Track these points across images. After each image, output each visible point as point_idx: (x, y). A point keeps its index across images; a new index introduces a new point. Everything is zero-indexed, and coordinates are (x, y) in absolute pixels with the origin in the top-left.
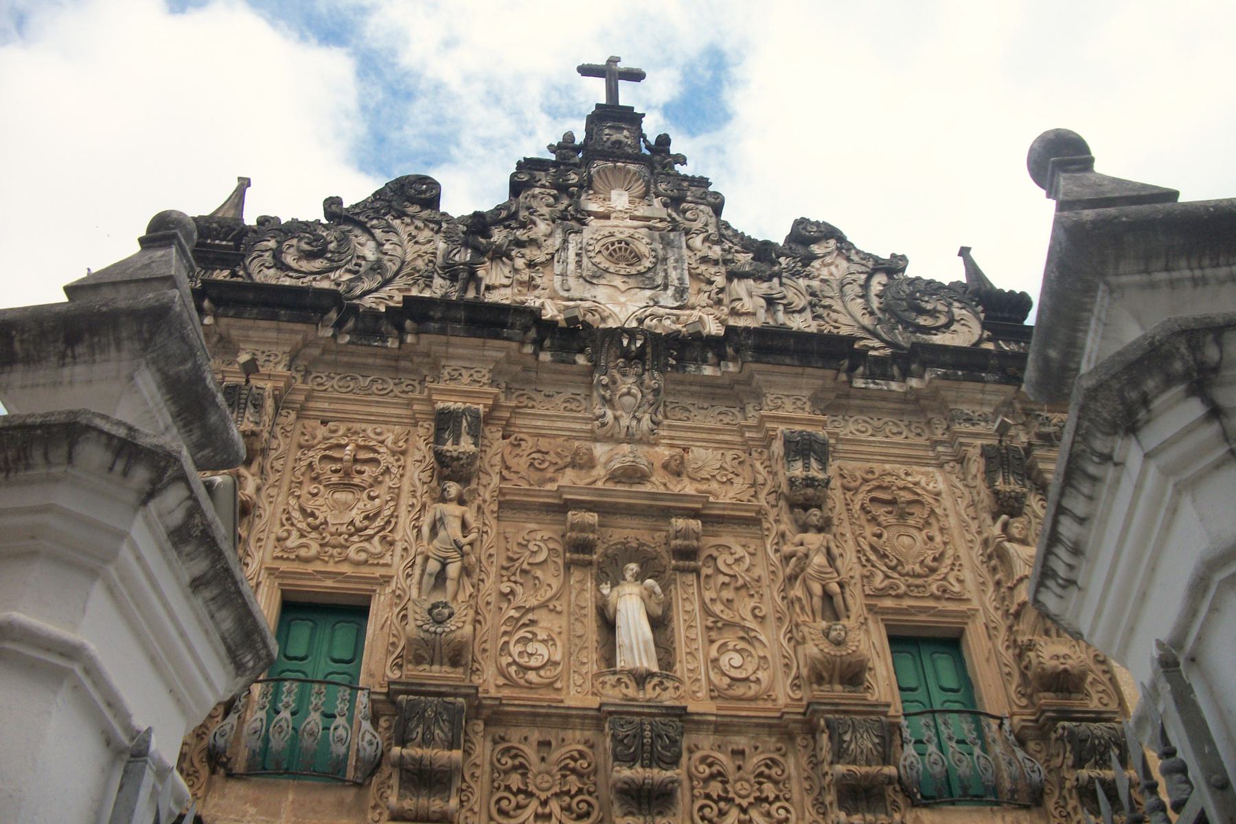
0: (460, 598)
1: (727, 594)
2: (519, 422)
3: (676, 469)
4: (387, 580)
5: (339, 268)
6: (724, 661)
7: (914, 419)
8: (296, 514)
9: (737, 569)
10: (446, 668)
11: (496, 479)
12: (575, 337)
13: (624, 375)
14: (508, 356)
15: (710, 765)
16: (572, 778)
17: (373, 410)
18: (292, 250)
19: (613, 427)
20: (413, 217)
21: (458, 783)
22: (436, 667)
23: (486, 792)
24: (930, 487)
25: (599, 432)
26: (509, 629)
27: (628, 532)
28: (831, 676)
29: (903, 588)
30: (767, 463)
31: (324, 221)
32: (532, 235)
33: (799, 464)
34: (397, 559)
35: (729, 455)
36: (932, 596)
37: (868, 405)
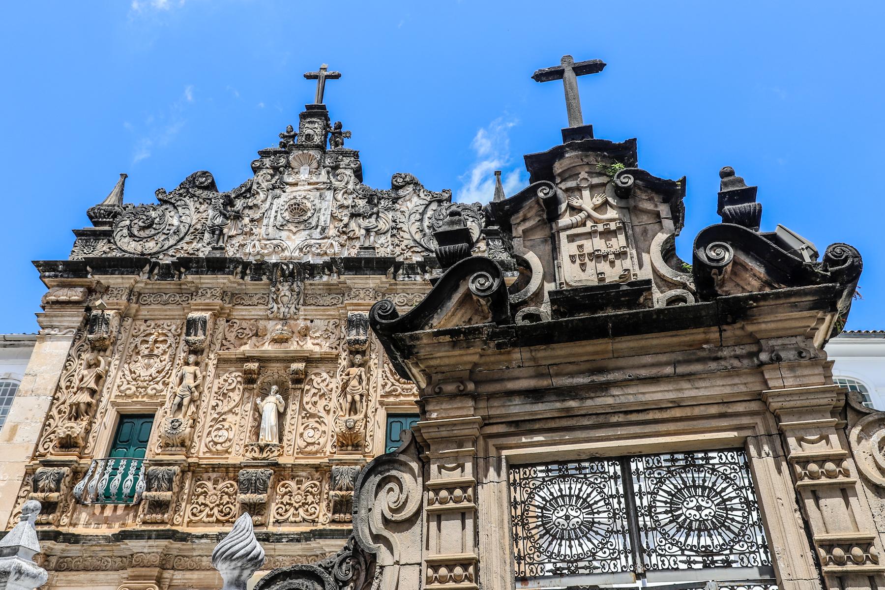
0: (189, 413)
6: (305, 435)
9: (323, 385)
12: (259, 269)
25: (271, 316)
26: (212, 424)
32: (255, 202)
33: (354, 332)
35: (332, 322)
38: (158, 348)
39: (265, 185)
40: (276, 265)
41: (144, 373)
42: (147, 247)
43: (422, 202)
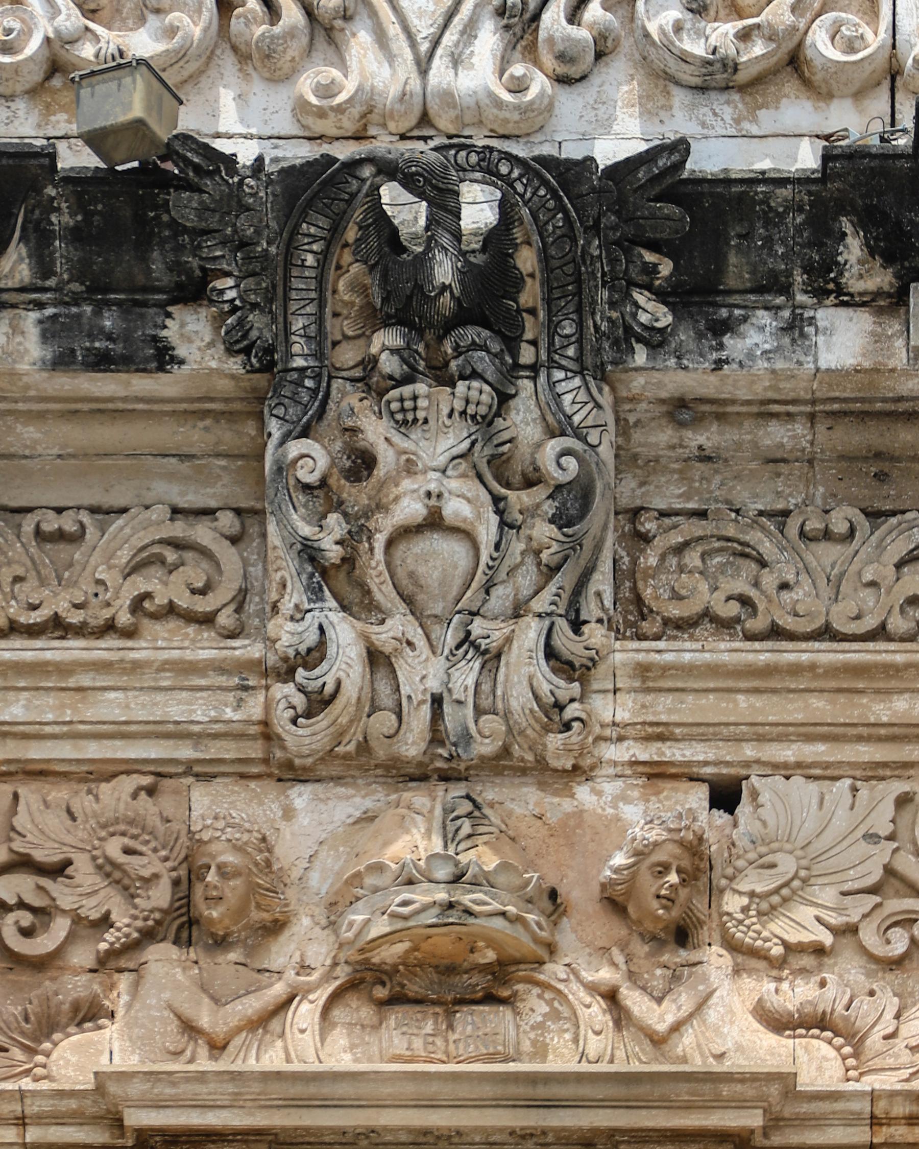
25: (304, 739)
40: (319, 190)
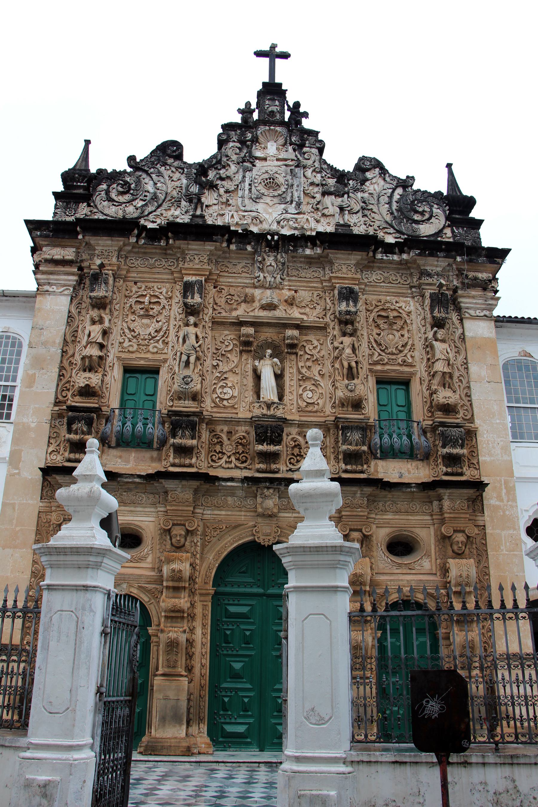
1: (309, 364)
2: (221, 280)
3: (290, 302)
4: (165, 361)
5: (136, 199)
7: (405, 272)
8: (127, 331)
10: (191, 402)
11: (211, 310)
13: (269, 256)
14: (216, 248)
15: (295, 441)
16: (240, 447)
17: (157, 276)
18: (114, 190)
19: (263, 281)
20: (170, 166)
21: (195, 451)
22: (186, 402)
23: (207, 453)
24: (406, 310)
25: (257, 284)
26: (216, 382)
27: (268, 334)
28: (348, 404)
29: (386, 360)
30: (332, 298)
31: (129, 170)
33: (344, 304)
34: (170, 350)
35: (316, 293)
36: (399, 364)
37: (383, 266)
38: (153, 309)
39: (234, 157)
41: (144, 332)
42: (127, 212)
43: (388, 186)
